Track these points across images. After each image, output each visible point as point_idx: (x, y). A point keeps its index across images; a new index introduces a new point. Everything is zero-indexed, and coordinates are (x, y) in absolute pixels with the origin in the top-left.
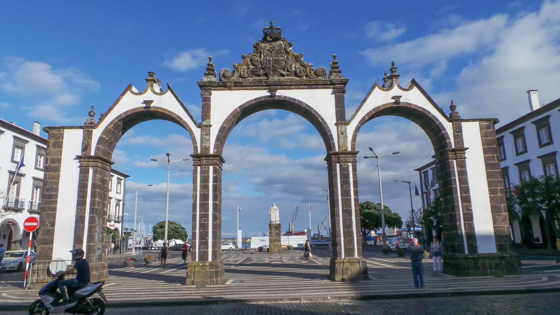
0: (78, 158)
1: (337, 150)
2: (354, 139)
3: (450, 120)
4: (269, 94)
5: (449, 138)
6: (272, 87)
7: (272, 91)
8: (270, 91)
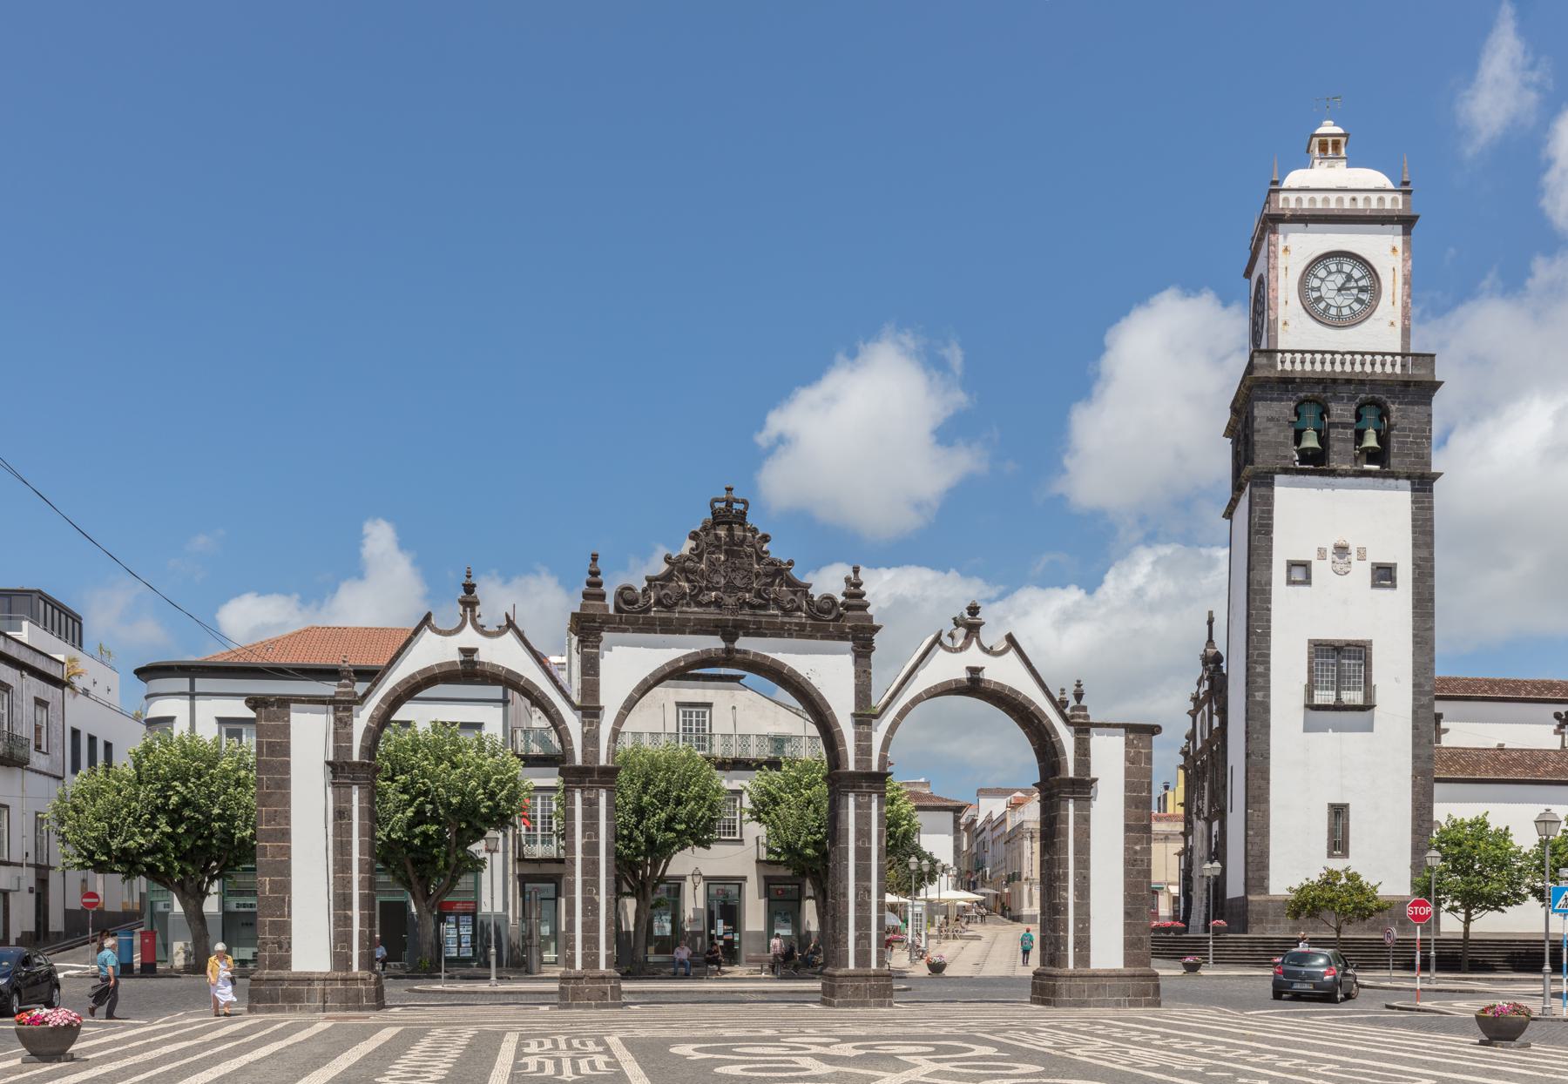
0: (328, 763)
1: (852, 767)
2: (886, 745)
3: (1067, 720)
4: (722, 645)
5: (1064, 754)
6: (729, 632)
7: (730, 637)
8: (724, 639)
